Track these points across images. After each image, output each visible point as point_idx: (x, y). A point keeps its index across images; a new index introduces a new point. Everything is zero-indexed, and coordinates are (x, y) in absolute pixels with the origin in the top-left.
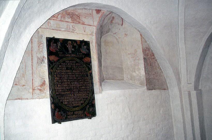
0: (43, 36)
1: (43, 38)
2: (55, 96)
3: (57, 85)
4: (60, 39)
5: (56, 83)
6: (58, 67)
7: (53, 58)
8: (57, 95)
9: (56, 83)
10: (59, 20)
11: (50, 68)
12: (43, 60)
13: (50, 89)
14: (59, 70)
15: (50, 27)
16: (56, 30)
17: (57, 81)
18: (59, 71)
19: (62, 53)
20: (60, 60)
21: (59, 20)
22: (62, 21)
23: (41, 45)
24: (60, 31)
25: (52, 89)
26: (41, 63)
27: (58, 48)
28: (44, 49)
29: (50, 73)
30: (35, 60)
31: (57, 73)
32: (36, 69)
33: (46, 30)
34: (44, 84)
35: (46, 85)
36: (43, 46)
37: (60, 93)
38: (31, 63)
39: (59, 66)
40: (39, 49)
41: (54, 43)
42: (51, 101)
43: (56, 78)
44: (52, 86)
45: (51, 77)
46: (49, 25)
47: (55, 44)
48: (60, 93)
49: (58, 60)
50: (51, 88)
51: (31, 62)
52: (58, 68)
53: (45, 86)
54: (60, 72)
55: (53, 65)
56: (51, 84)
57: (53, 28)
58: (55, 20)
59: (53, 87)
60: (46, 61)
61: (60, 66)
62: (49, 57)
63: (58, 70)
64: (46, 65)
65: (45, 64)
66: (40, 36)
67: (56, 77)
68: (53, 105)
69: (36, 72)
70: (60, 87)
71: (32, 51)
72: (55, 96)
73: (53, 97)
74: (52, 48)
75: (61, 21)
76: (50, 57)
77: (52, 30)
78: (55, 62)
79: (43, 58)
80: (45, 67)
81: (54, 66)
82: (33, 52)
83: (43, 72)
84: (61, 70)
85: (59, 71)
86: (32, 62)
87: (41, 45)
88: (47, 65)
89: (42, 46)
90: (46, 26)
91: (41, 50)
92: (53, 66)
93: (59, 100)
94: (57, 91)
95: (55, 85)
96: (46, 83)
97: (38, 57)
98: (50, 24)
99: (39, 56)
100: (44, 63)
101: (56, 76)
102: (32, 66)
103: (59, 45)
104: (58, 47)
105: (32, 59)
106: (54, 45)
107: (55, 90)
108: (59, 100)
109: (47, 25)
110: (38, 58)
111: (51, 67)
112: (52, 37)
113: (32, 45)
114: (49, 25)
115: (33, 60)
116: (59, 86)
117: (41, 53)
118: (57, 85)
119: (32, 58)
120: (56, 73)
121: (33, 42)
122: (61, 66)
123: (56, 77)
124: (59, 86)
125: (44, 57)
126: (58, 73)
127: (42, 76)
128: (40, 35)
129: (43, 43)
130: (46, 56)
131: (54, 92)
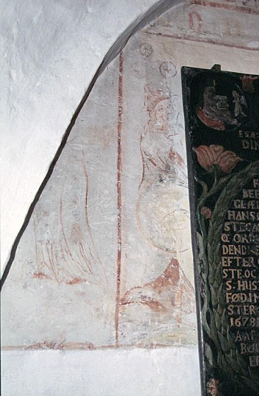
0: (170, 67)
1: (168, 75)
2: (225, 335)
3: (234, 283)
4: (242, 75)
5: (229, 273)
6: (240, 196)
7: (210, 155)
8: (234, 330)
9: (229, 273)
10: (237, 8)
11: (201, 202)
12: (168, 169)
13: (200, 301)
14: (241, 210)
15: (199, 33)
16: (225, 45)
17: (234, 261)
18: (242, 216)
19: (253, 134)
20: (248, 164)
21: (237, 8)
22: (249, 11)
23: (162, 103)
24: (243, 48)
25: (210, 303)
26: (161, 181)
27: (236, 115)
28: (175, 121)
29: (200, 225)
30: (133, 167)
31: (231, 226)
32: (138, 206)
33: (184, 43)
34: (171, 274)
35: (181, 281)
36: (170, 106)
37: (248, 322)
38: (116, 181)
39: (241, 194)
40: (153, 118)
41: (219, 91)
42: (206, 360)
43: (227, 249)
44: (212, 289)
45: (205, 240)
46: (196, 26)
47: (223, 98)
48: (248, 322)
49: (239, 166)
50: (205, 296)
51: (116, 176)
52: (238, 203)
53: (174, 284)
54: (247, 221)
55: (214, 188)
56: (204, 276)
57: (212, 37)
58: (219, 6)
59: (213, 293)
60: (182, 171)
61: (245, 192)
62: (197, 153)
63: (237, 210)
64: (184, 192)
65: (177, 182)
66: (156, 65)
67: (227, 244)
68: (213, 384)
69: (138, 219)
70: (247, 292)
71: (119, 127)
72: (225, 335)
73: (215, 339)
74: (208, 116)
75: (243, 9)
76: (199, 151)
77: (206, 45)
78: (222, 174)
79: (171, 157)
80: (177, 199)
81: (219, 192)
82: (122, 133)
83: (170, 222)
84: (250, 210)
85: (242, 216)
86: (119, 175)
87: (159, 104)
88: (186, 191)
89: (165, 106)
90: (182, 29)
91: (159, 124)
92: (212, 192)
93: (246, 357)
94: (235, 309)
95: (225, 280)
96: (181, 274)
97: (144, 153)
98: (200, 20)
99: (151, 151)
100: (173, 181)
101: (230, 238)
102: (119, 191)
103: (239, 103)
104: (237, 108)
105: (119, 163)
106: (218, 100)
107: (227, 306)
108: (246, 357)
109: (186, 25)
110: (148, 160)
111: (206, 194)
112: (210, 68)
113: (120, 100)
114: (196, 26)
115: (124, 166)
116: (242, 285)
117: (162, 136)
118: (234, 283)
119: (119, 159)
120: (227, 224)
121: (124, 89)
122: (250, 191)
123: (227, 244)
124: (242, 285)
125: (172, 155)
126: (238, 227)
127: (166, 240)
128: (158, 61)
129: (167, 94)
130: (182, 151)
131: (220, 315)
